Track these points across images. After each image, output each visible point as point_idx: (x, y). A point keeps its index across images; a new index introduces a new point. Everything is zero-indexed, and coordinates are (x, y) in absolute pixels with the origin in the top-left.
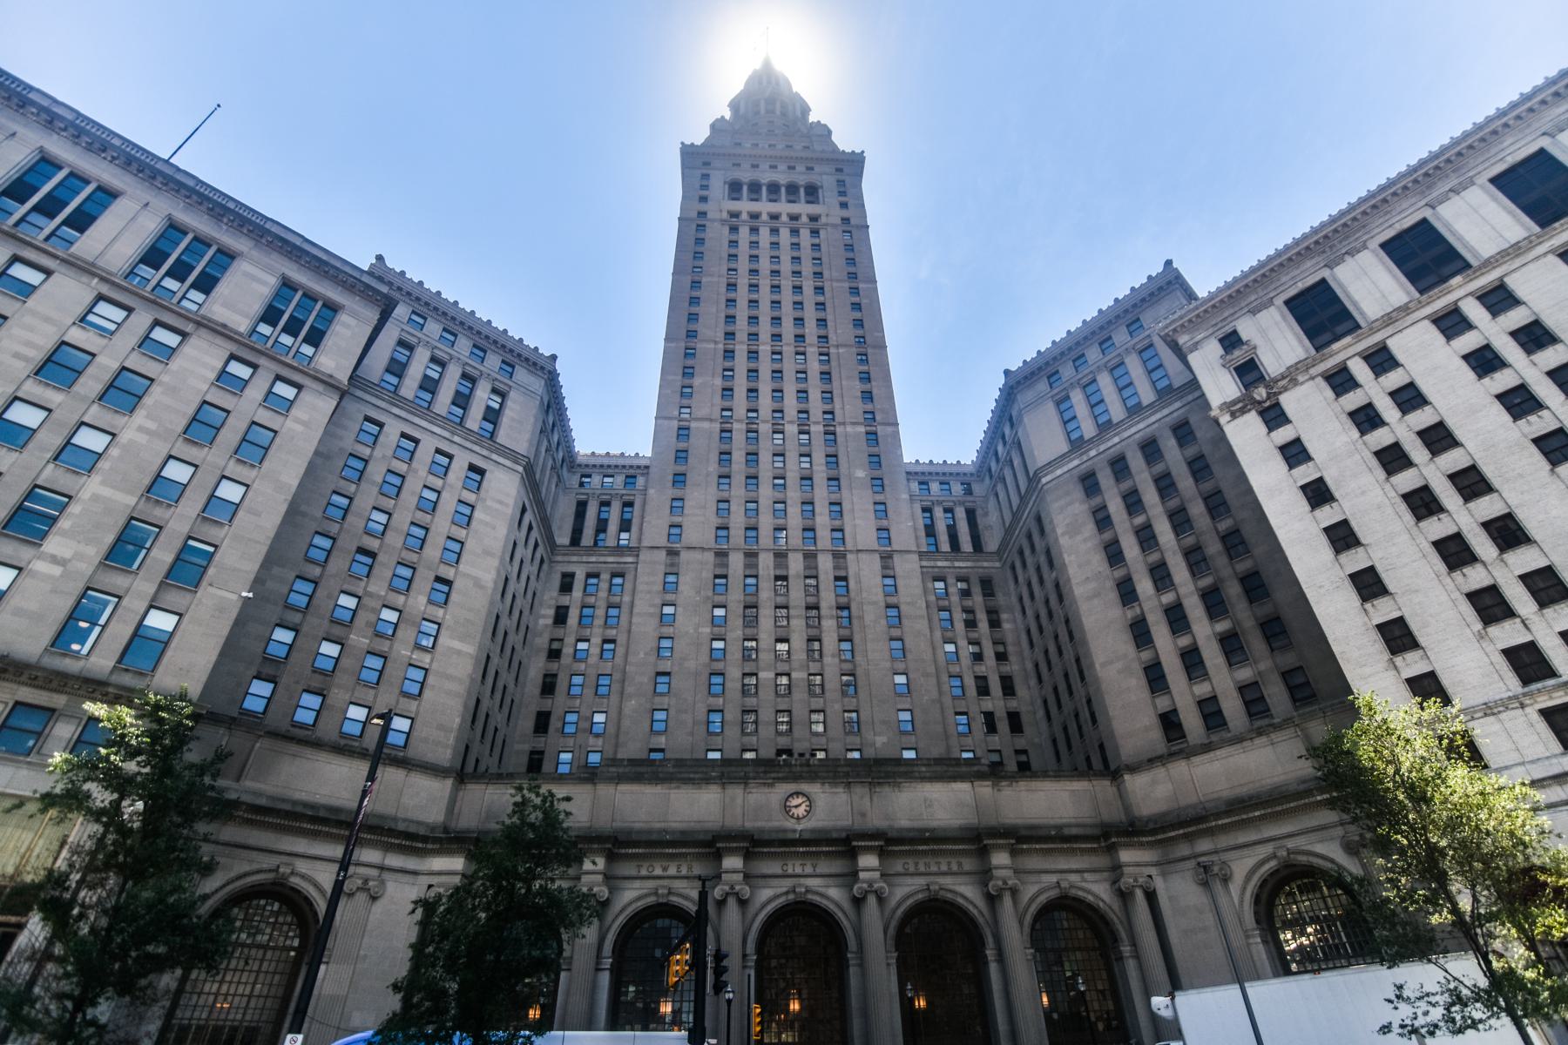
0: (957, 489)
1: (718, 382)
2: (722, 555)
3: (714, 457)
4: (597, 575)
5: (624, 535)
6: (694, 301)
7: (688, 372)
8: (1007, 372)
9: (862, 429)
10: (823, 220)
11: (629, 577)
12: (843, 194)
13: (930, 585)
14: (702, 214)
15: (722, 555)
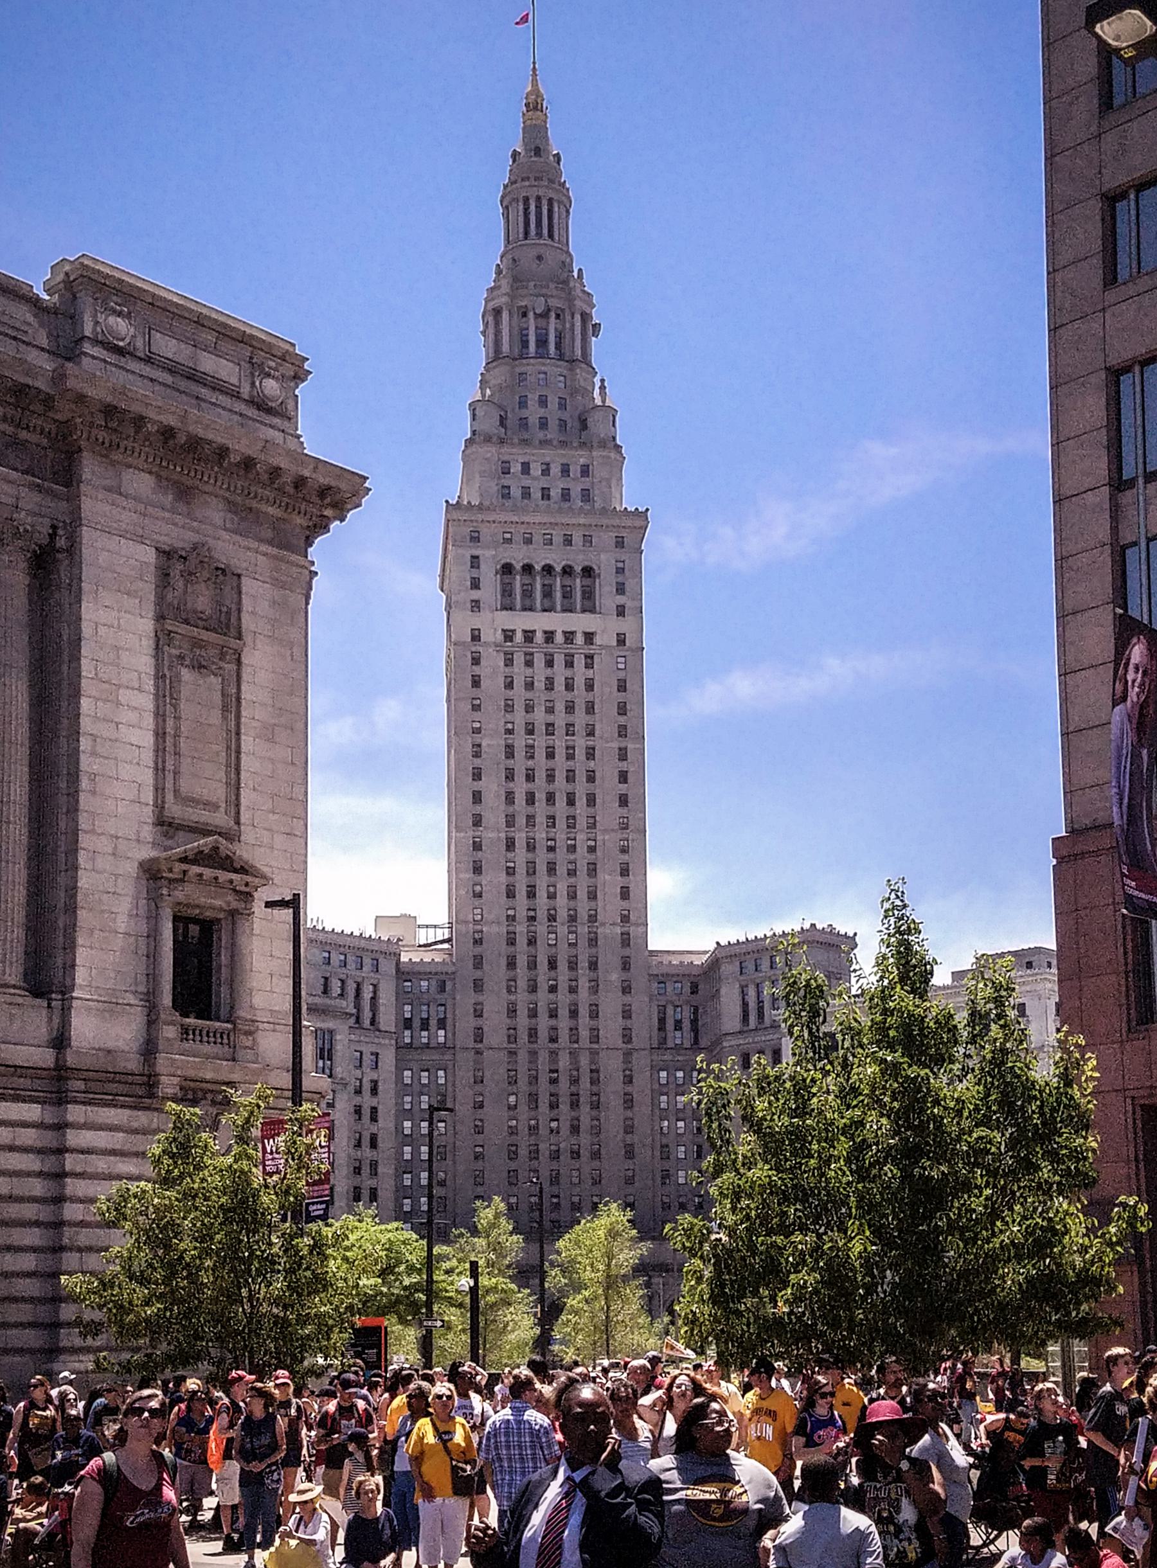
0: (687, 989)
1: (503, 878)
2: (513, 1053)
3: (503, 962)
4: (427, 1070)
5: (441, 1033)
6: (477, 775)
7: (477, 869)
8: (718, 943)
9: (618, 930)
10: (598, 640)
11: (449, 1071)
12: (621, 589)
13: (655, 1076)
14: (476, 637)
15: (513, 1053)
